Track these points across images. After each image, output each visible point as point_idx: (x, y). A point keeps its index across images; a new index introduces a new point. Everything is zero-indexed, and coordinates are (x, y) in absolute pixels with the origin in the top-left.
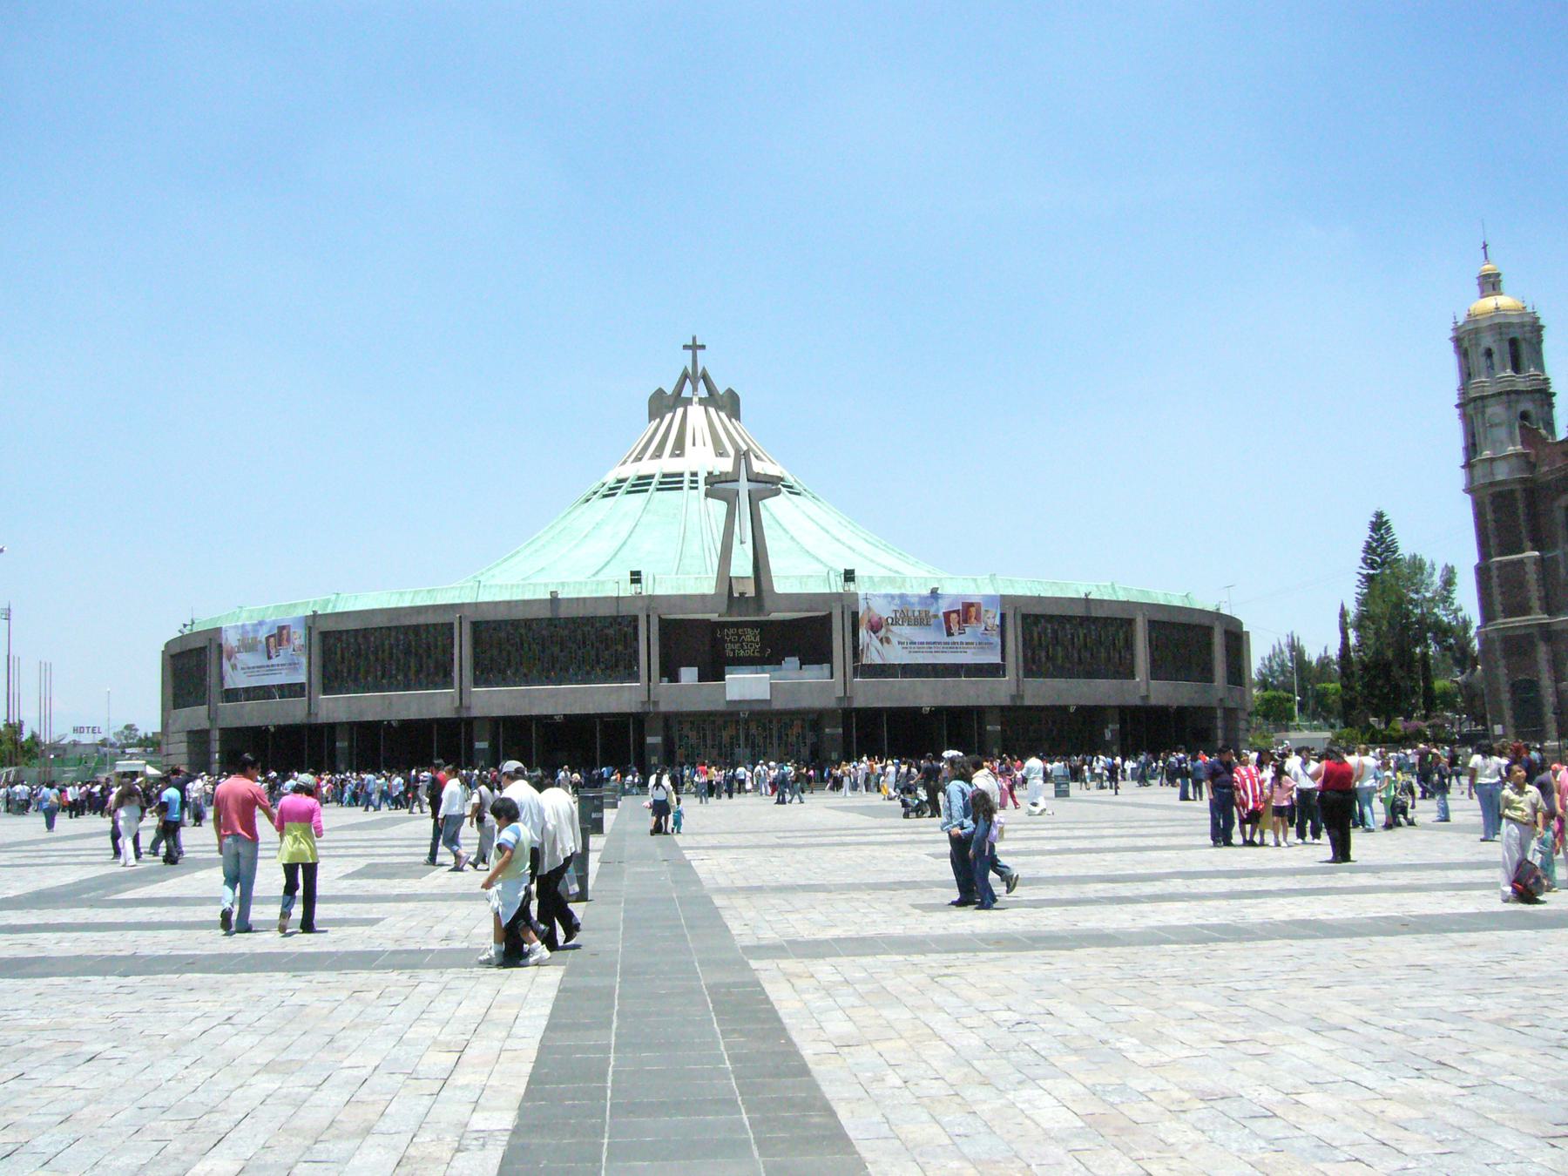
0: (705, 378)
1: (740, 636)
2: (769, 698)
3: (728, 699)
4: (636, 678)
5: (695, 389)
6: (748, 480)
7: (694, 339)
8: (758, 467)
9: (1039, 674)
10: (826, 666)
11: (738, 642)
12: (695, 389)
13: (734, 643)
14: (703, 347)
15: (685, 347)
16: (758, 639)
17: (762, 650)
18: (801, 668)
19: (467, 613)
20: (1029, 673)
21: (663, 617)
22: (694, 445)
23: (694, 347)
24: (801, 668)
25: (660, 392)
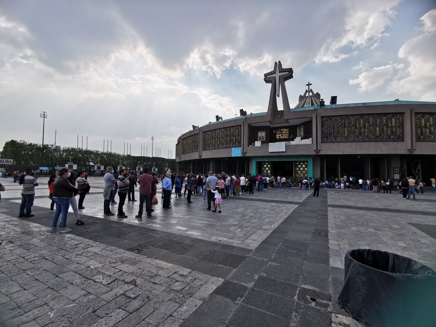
0: (311, 91)
1: (281, 132)
2: (284, 150)
3: (270, 151)
4: (241, 147)
5: (309, 94)
6: (279, 72)
7: (309, 82)
8: (284, 66)
9: (424, 141)
10: (310, 139)
11: (281, 134)
12: (309, 94)
13: (280, 134)
14: (311, 84)
15: (307, 85)
16: (288, 132)
17: (289, 136)
18: (301, 140)
19: (202, 129)
20: (419, 139)
21: (253, 125)
22: (306, 105)
23: (309, 85)
24: (301, 140)
25: (301, 95)
